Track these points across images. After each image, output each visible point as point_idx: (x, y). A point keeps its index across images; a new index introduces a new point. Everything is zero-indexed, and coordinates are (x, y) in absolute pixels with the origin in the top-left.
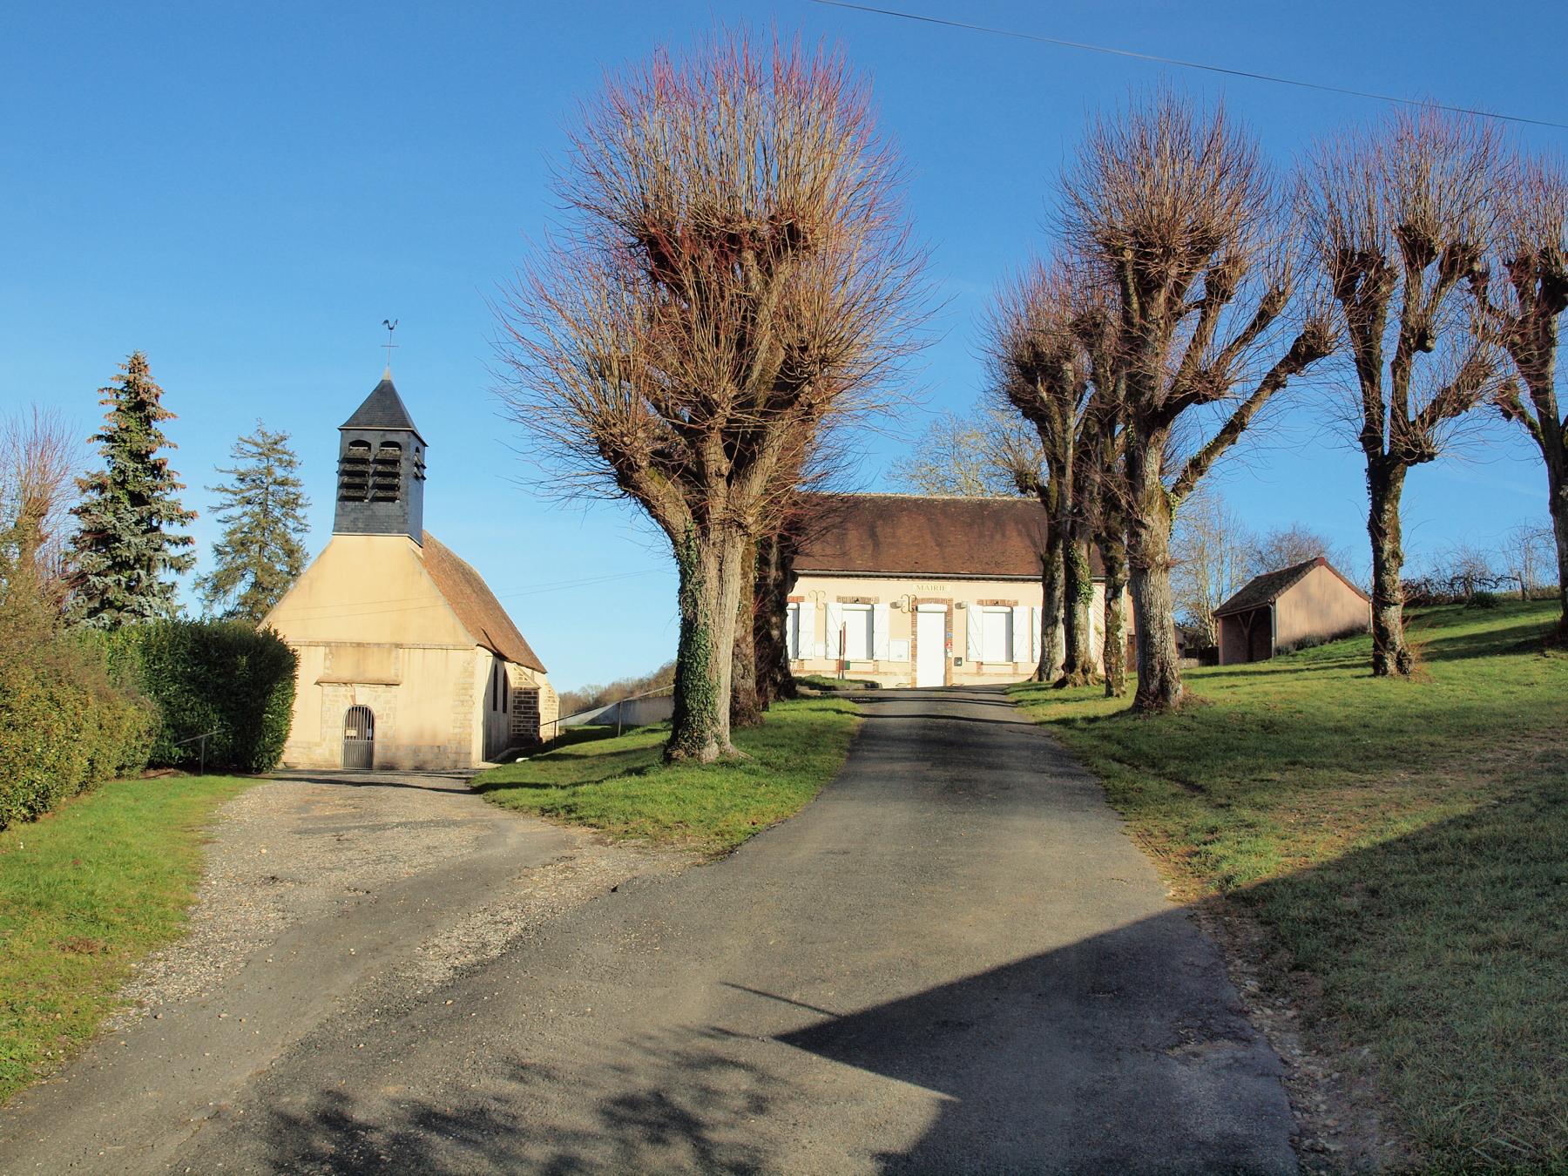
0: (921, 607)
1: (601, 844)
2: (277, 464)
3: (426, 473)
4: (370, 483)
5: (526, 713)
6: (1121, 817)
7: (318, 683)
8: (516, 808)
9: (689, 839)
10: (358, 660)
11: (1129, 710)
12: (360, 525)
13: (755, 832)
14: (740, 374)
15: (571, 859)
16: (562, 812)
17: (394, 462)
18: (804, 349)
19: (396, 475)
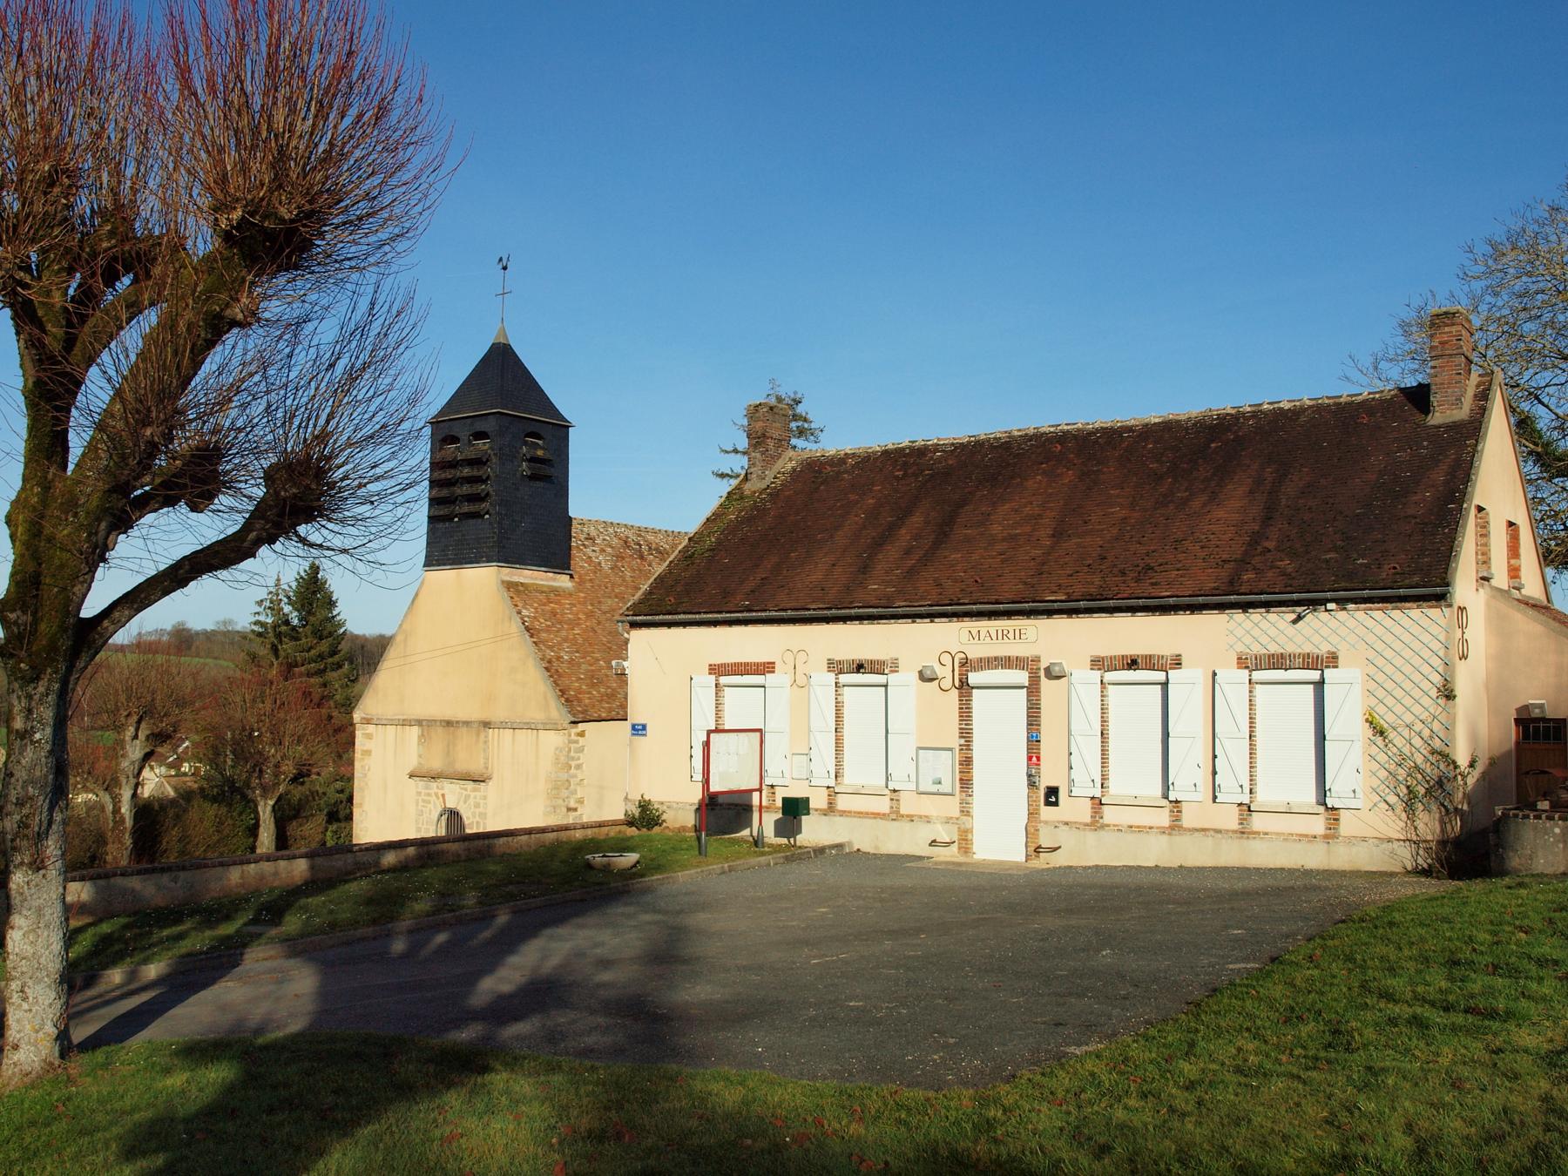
0: (973, 678)
10: (448, 745)
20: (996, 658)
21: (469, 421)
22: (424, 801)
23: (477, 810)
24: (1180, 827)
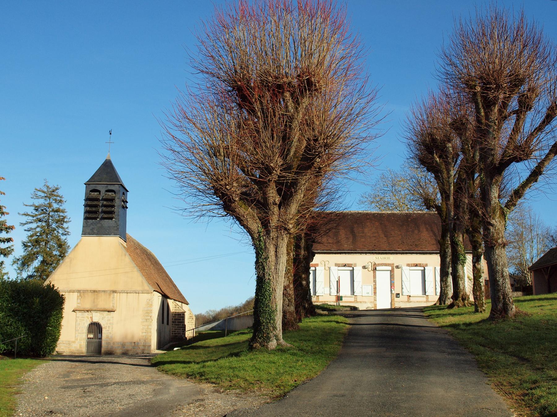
0: (378, 268)
1: (218, 392)
2: (54, 201)
3: (128, 205)
4: (100, 210)
5: (178, 325)
6: (486, 376)
7: (74, 311)
8: (174, 374)
9: (262, 389)
10: (94, 299)
11: (487, 319)
12: (95, 231)
13: (296, 385)
14: (284, 154)
15: (202, 400)
16: (198, 376)
17: (112, 200)
18: (316, 140)
19: (113, 206)
20: (383, 264)
21: (106, 185)
22: (80, 320)
23: (109, 322)
24: (429, 301)
